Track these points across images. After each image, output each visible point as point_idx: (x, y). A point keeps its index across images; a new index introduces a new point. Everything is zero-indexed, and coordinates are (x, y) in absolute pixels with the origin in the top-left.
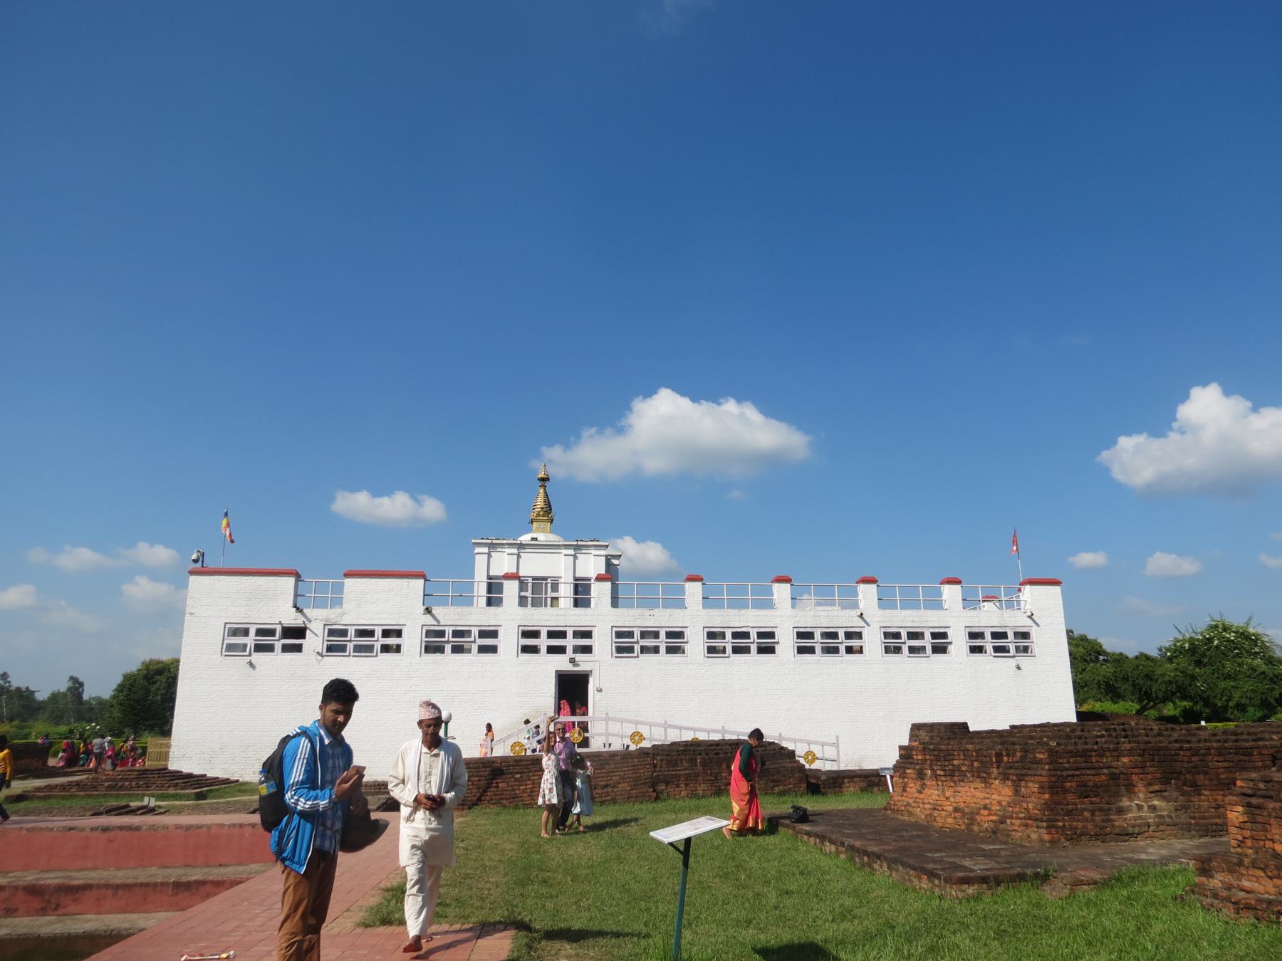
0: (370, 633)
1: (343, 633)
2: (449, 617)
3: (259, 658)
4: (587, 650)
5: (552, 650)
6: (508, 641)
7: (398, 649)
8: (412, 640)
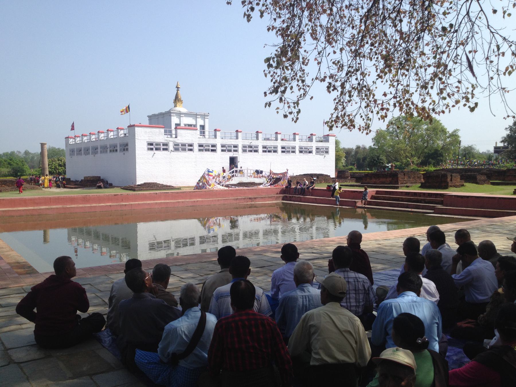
0: (185, 145)
1: (178, 145)
2: (203, 141)
3: (157, 152)
4: (235, 151)
5: (230, 151)
6: (219, 148)
7: (191, 150)
8: (196, 148)
